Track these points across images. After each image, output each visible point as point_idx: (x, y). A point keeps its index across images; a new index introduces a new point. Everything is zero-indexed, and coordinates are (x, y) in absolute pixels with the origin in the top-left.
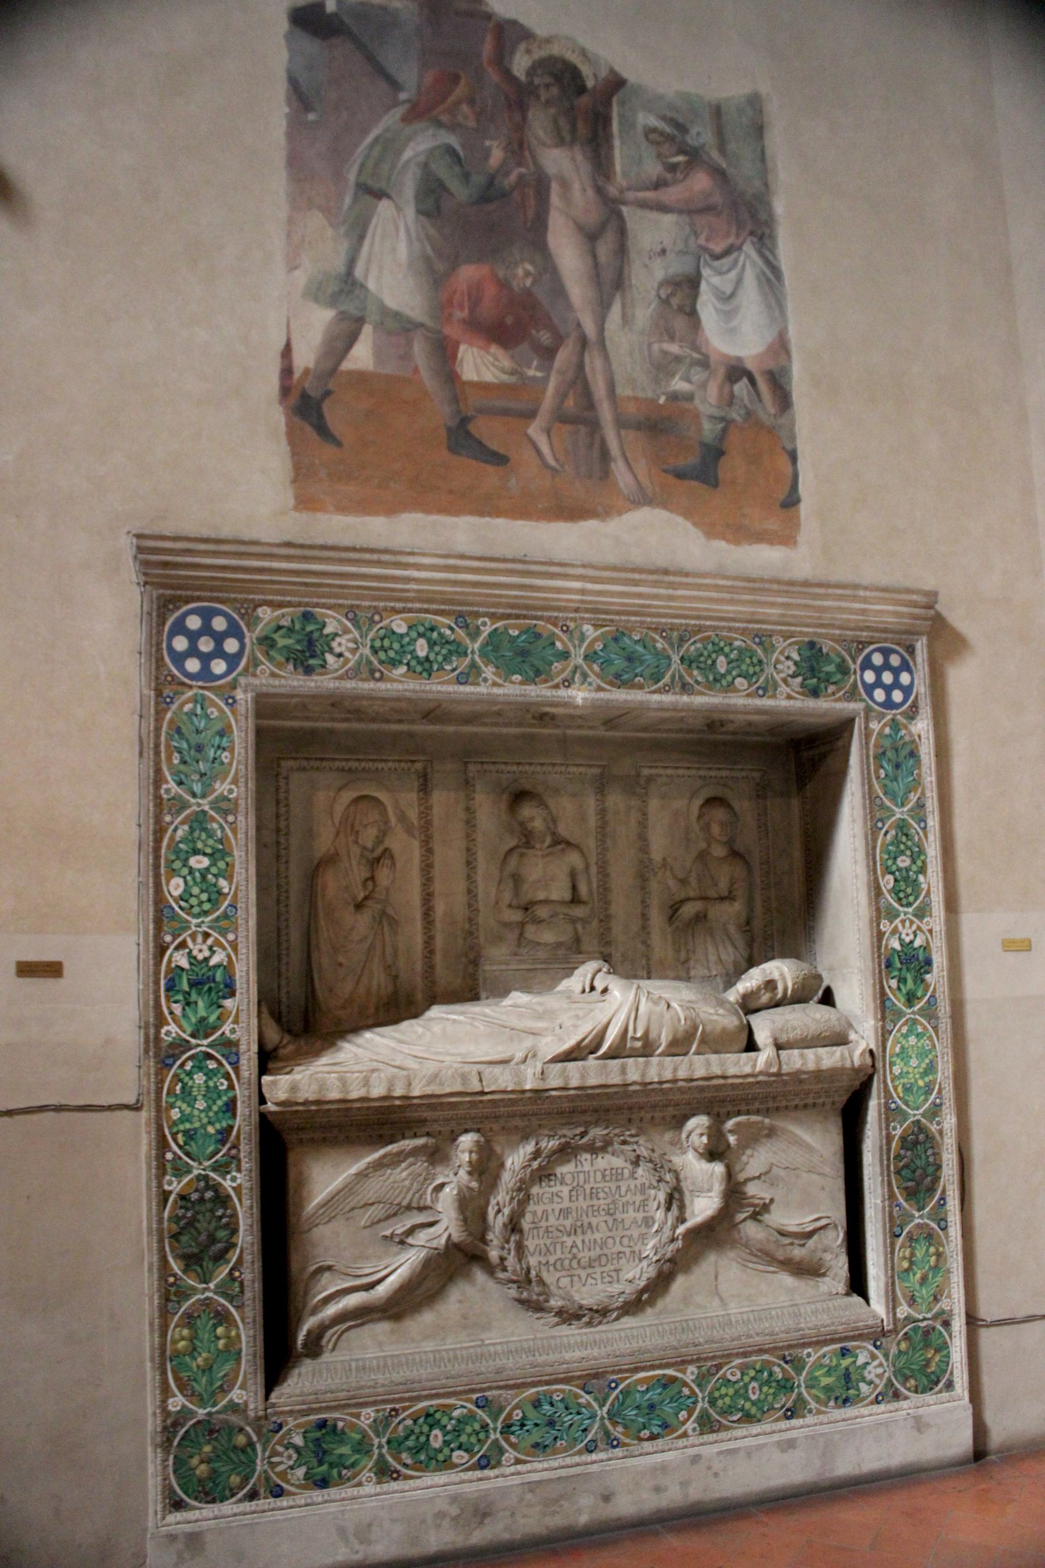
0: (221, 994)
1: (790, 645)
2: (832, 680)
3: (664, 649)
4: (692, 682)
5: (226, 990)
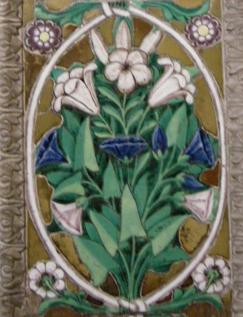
0: (180, 178)
5: (195, 169)
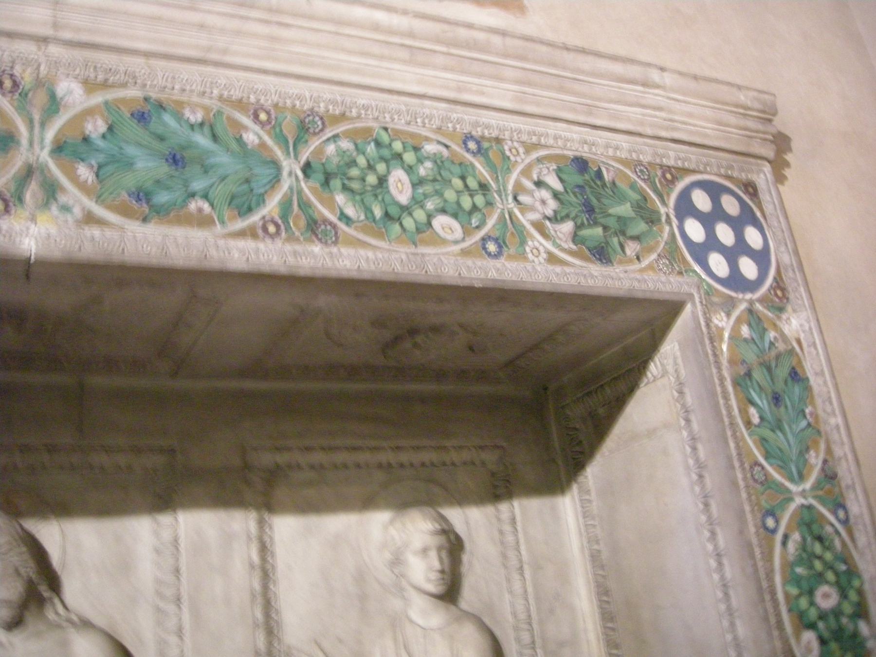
1: (539, 160)
3: (263, 145)
4: (333, 218)
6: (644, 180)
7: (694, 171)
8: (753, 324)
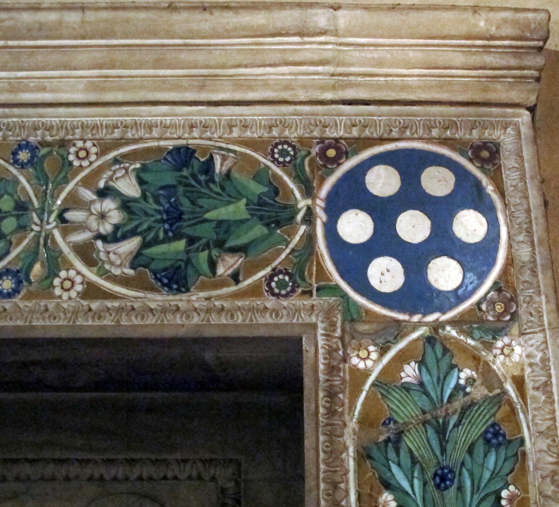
1: (116, 161)
2: (230, 243)
6: (283, 165)
7: (382, 140)
8: (430, 360)
